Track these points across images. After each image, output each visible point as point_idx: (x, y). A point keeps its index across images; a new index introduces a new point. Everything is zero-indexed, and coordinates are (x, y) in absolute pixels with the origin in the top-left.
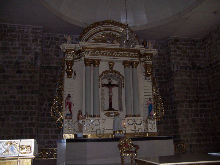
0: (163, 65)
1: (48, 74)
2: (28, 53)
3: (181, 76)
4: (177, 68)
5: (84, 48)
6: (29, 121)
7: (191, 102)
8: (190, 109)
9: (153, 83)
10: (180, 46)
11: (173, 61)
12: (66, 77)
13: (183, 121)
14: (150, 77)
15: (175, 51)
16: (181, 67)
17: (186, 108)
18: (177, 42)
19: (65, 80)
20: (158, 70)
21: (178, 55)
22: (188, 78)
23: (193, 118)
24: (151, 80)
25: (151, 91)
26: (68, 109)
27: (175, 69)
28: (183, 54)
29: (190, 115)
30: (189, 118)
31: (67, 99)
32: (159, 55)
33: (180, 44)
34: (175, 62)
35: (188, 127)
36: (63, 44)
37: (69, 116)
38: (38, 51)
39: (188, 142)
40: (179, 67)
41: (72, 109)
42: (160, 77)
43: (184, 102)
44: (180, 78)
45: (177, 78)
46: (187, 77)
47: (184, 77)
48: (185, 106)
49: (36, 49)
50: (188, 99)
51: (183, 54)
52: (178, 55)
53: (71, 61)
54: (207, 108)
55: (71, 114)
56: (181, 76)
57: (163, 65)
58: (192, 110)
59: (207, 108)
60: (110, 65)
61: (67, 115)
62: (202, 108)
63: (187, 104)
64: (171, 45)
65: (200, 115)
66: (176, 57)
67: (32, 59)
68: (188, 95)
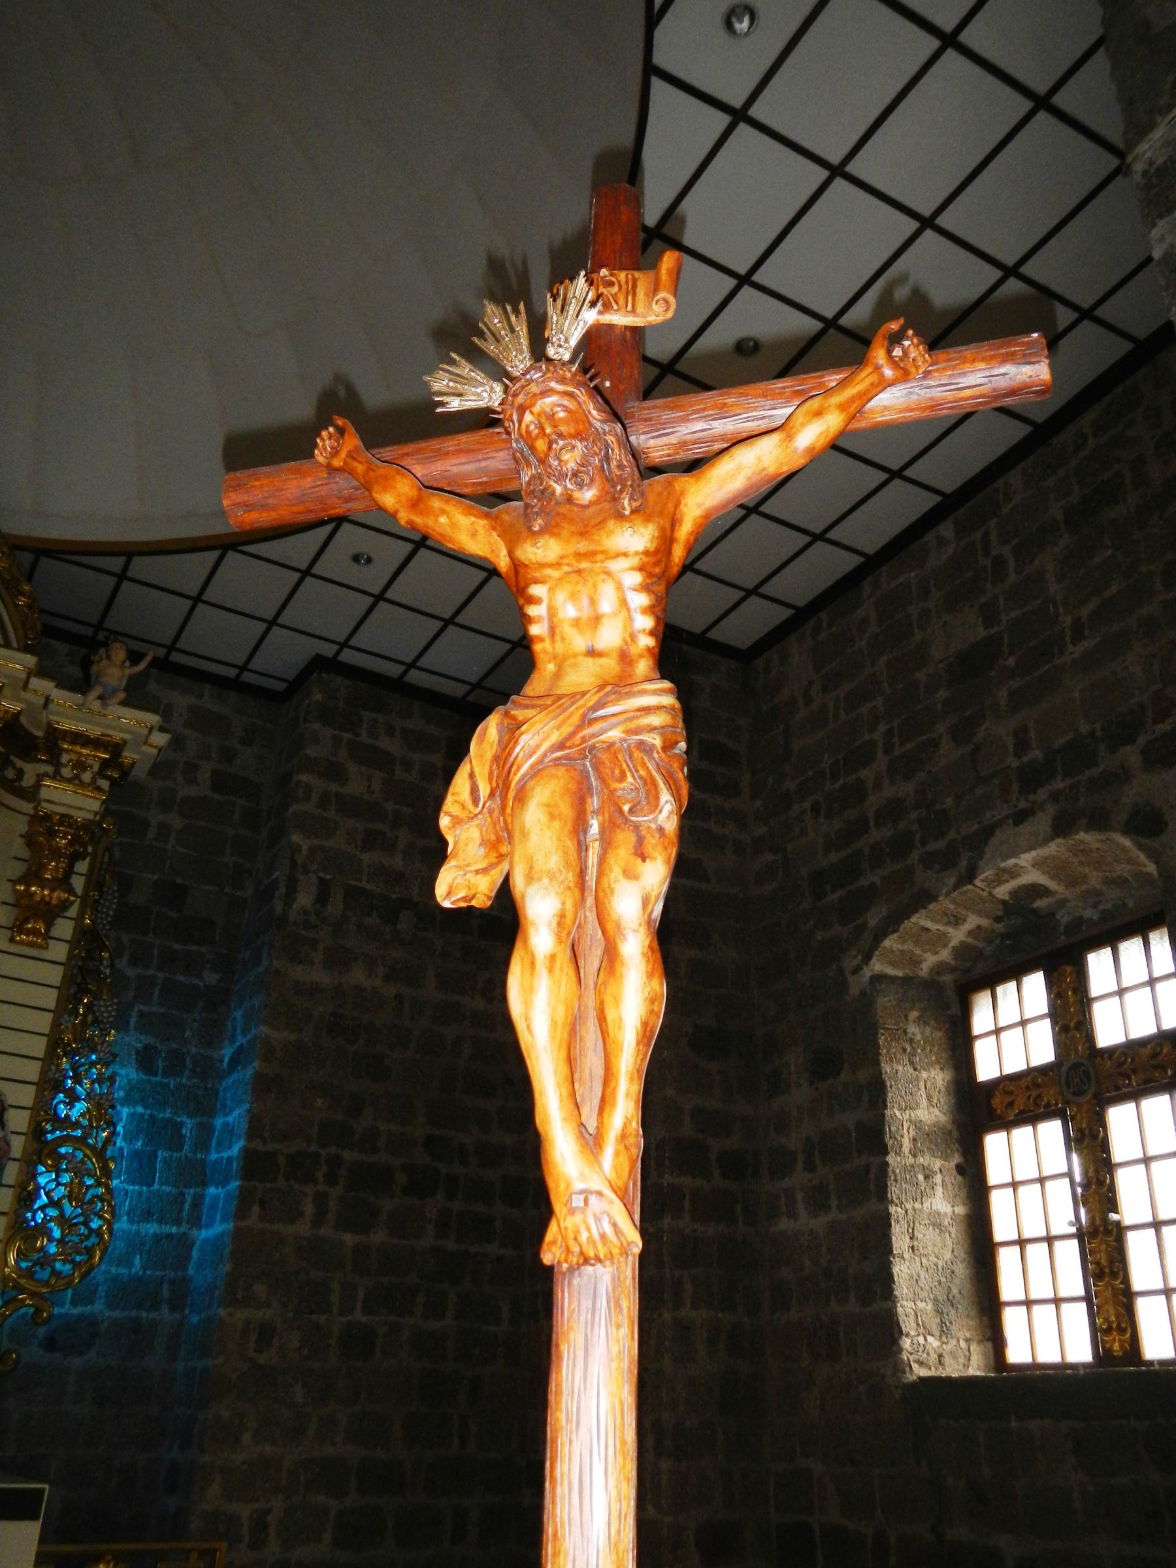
4: (323, 897)
8: (349, 1239)
10: (384, 743)
11: (295, 837)
13: (266, 1333)
14: (64, 928)
15: (334, 772)
17: (318, 1220)
18: (367, 715)
22: (390, 990)
23: (359, 1316)
24: (59, 951)
25: (38, 1047)
27: (304, 900)
28: (390, 806)
29: (336, 1286)
30: (323, 1319)
32: (219, 782)
33: (391, 731)
34: (312, 851)
35: (299, 1393)
39: (255, 1544)
42: (177, 947)
44: (324, 978)
45: (298, 973)
46: (387, 978)
47: (358, 976)
48: (309, 1209)
51: (390, 806)
54: (493, 1249)
59: (493, 1249)
62: (451, 1245)
64: (317, 726)
65: (421, 1299)
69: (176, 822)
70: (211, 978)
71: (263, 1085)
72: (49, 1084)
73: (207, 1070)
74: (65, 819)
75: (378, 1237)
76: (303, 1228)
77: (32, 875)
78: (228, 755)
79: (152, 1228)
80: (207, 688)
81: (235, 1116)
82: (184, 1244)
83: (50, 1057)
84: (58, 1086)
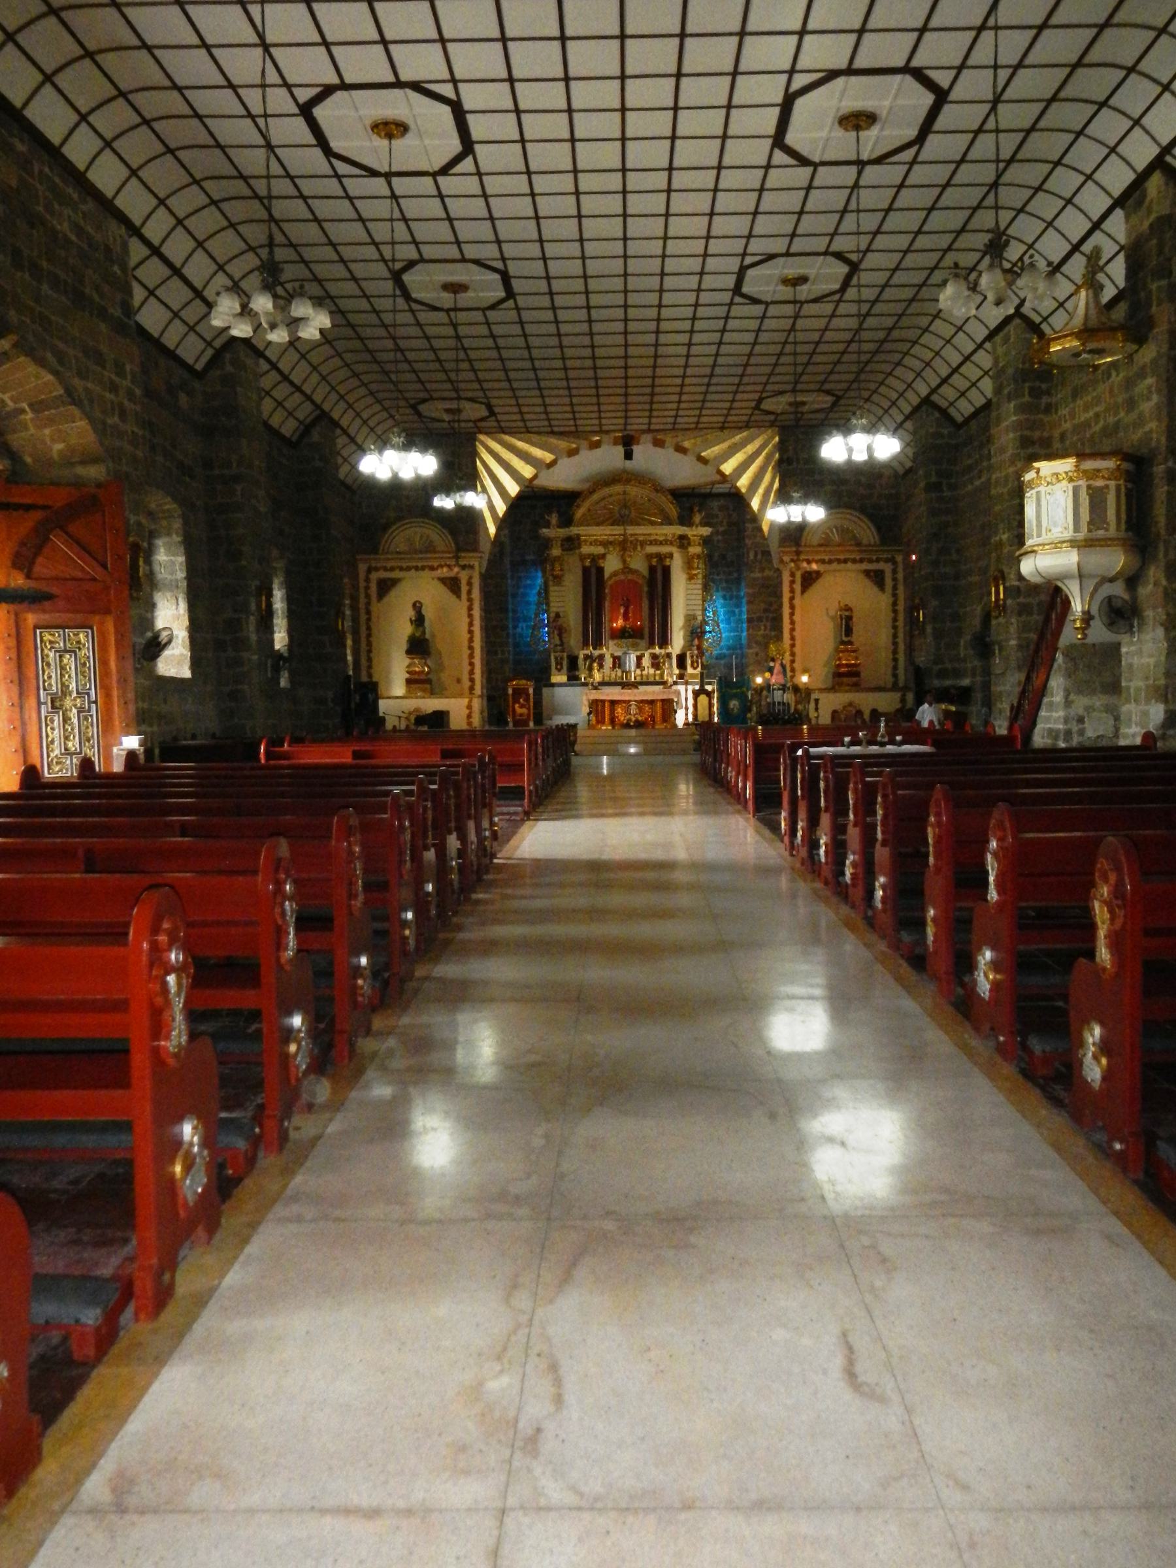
5: (578, 536)
9: (706, 588)
12: (551, 583)
13: (757, 654)
14: (700, 576)
19: (552, 589)
24: (700, 581)
26: (557, 638)
27: (752, 556)
32: (730, 524)
36: (545, 530)
41: (564, 635)
55: (562, 644)
69: (720, 537)
70: (735, 575)
71: (749, 602)
72: (704, 610)
73: (738, 598)
76: (762, 632)
78: (730, 516)
81: (744, 609)
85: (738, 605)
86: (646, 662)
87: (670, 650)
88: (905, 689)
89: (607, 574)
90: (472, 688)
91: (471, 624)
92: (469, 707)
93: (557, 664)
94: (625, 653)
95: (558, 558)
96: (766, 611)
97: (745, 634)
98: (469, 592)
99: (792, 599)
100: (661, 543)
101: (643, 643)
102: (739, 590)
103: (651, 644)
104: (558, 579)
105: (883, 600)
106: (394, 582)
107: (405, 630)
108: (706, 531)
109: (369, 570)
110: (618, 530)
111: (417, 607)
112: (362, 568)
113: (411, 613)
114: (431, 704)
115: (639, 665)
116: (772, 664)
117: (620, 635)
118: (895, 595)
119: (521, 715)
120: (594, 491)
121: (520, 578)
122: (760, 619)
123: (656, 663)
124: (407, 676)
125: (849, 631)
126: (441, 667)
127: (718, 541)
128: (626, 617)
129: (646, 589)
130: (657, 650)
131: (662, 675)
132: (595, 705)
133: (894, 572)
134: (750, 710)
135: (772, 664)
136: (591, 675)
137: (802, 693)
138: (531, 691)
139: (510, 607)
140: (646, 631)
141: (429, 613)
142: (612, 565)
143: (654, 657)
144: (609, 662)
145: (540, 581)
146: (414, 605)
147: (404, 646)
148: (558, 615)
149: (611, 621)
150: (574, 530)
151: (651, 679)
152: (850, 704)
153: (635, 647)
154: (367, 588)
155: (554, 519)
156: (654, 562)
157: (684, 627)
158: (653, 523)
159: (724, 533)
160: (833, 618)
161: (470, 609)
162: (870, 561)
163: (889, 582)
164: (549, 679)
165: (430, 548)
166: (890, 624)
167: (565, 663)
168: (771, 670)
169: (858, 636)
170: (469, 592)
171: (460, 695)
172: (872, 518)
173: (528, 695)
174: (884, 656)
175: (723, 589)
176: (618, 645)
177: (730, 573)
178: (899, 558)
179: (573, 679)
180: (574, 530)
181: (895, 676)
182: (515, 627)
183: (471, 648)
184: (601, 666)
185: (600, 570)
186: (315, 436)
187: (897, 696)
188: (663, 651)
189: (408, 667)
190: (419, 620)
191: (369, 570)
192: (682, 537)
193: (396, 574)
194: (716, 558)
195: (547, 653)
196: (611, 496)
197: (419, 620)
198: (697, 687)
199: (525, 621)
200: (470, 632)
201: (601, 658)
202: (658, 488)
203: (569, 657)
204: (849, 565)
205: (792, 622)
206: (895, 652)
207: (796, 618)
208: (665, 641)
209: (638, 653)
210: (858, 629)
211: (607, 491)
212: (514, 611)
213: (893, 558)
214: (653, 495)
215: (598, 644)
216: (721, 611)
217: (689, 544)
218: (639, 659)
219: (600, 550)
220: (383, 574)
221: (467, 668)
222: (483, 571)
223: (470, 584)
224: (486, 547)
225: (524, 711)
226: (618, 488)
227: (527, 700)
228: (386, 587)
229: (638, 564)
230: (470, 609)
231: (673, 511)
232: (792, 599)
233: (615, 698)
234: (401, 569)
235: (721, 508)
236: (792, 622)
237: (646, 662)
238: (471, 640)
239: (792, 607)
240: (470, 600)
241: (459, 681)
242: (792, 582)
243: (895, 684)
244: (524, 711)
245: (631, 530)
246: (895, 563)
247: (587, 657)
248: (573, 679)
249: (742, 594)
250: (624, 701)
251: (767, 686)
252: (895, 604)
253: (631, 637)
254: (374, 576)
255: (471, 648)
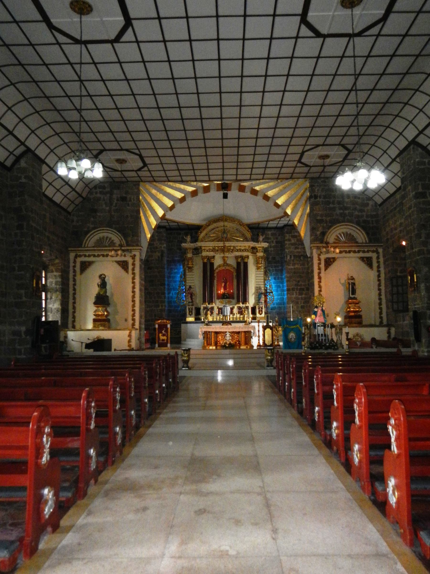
0: (280, 252)
1: (173, 267)
2: (155, 252)
3: (294, 264)
4: (291, 257)
5: (201, 247)
6: (160, 308)
7: (303, 290)
8: (300, 296)
9: (265, 273)
12: (187, 271)
14: (263, 268)
15: (289, 240)
16: (295, 256)
17: (296, 295)
18: (293, 231)
19: (187, 274)
20: (275, 258)
21: (292, 244)
22: (301, 267)
23: (302, 304)
24: (263, 270)
25: (263, 281)
26: (190, 298)
27: (289, 258)
31: (188, 290)
32: (277, 242)
37: (191, 304)
38: (163, 249)
40: (293, 257)
41: (194, 297)
43: (294, 290)
44: (292, 267)
47: (296, 266)
48: (295, 294)
49: (161, 247)
50: (299, 287)
52: (292, 244)
53: (191, 258)
55: (192, 302)
56: (294, 264)
57: (280, 252)
58: (302, 298)
60: (224, 260)
61: (189, 302)
63: (298, 291)
66: (290, 246)
67: (159, 257)
68: (300, 284)
69: (272, 249)
70: (280, 268)
71: (288, 281)
72: (265, 284)
73: (282, 279)
74: (260, 256)
75: (303, 296)
76: (294, 296)
77: (258, 263)
78: (277, 238)
79: (279, 297)
80: (273, 230)
81: (285, 284)
82: (283, 298)
83: (264, 282)
84: (266, 284)
85: (282, 283)
86: (235, 311)
87: (247, 305)
88: (389, 326)
89: (215, 267)
90: (133, 325)
91: (134, 288)
92: (130, 336)
93: (189, 312)
94: (224, 306)
95: (191, 258)
96: (296, 285)
97: (285, 297)
98: (133, 269)
99: (319, 273)
100: (243, 251)
101: (234, 301)
102: (282, 275)
103: (238, 302)
104: (191, 269)
105: (372, 274)
106: (90, 263)
107: (95, 290)
108: (265, 245)
109: (76, 257)
110: (221, 244)
111: (102, 278)
112: (72, 256)
113: (98, 281)
114: (105, 334)
115: (232, 312)
116: (316, 310)
117: (223, 297)
118: (379, 271)
119: (163, 340)
120: (209, 225)
121: (172, 269)
122: (293, 289)
123: (241, 312)
124: (94, 317)
125: (354, 292)
126: (116, 312)
127: (271, 250)
128: (225, 288)
129: (235, 274)
130: (241, 305)
131: (244, 318)
132: (206, 334)
133: (378, 258)
134: (303, 339)
135: (316, 310)
136: (206, 318)
137: (339, 328)
138: (169, 326)
139: (166, 283)
140: (235, 296)
141: (110, 281)
142: (218, 261)
143: (239, 308)
144: (216, 311)
145: (182, 270)
146: (100, 276)
147: (93, 300)
148: (190, 287)
149: (218, 290)
150: (199, 244)
151: (238, 320)
152: (357, 335)
153: (230, 303)
154: (74, 267)
155: (189, 238)
156: (239, 260)
157: (254, 293)
158: (238, 241)
159: (274, 247)
160: (343, 284)
161: (133, 278)
162: (364, 252)
163: (375, 265)
164: (185, 319)
165: (112, 244)
166: (376, 287)
167: (194, 312)
168: (315, 313)
169: (359, 295)
170: (133, 269)
171: (124, 329)
172: (364, 228)
173: (167, 328)
174: (374, 306)
175: (274, 275)
176: (221, 302)
177: (278, 267)
178: (380, 250)
179: (198, 320)
180: (199, 244)
181: (381, 318)
182: (169, 293)
183: (133, 301)
184: (212, 313)
185: (212, 264)
186: (23, 163)
187: (385, 329)
188: (244, 305)
189: (95, 312)
190: (103, 285)
191: (76, 257)
192: (253, 248)
193: (92, 259)
194: (270, 259)
195: (185, 306)
196: (218, 227)
197: (103, 285)
198: (265, 324)
199: (174, 290)
200: (133, 292)
201: (212, 308)
202: (241, 224)
203: (196, 308)
204: (352, 254)
205: (320, 287)
206: (380, 304)
207: (322, 284)
208: (245, 300)
209: (231, 306)
210: (358, 291)
211: (215, 225)
212: (168, 285)
213: (377, 250)
214: (239, 227)
215: (211, 301)
216: (274, 285)
217: (257, 251)
218: (232, 309)
219: (211, 254)
220: (83, 259)
221: (131, 313)
222: (143, 257)
223: (133, 264)
224: (145, 245)
225: (165, 338)
226: (221, 224)
227: (166, 331)
228: (85, 266)
229: (232, 262)
230: (133, 278)
231: (249, 235)
232: (319, 273)
233: (218, 330)
234: (94, 256)
235: (272, 234)
236: (320, 287)
237: (235, 311)
238: (133, 297)
239: (320, 278)
240: (134, 274)
241: (126, 320)
242: (319, 264)
243: (381, 322)
244: (165, 338)
245: (227, 244)
246: (378, 253)
247: (205, 308)
248: (198, 320)
249: (284, 276)
250: (223, 332)
251: (314, 324)
252: (379, 276)
253: (227, 298)
254: (79, 260)
255: (133, 301)
